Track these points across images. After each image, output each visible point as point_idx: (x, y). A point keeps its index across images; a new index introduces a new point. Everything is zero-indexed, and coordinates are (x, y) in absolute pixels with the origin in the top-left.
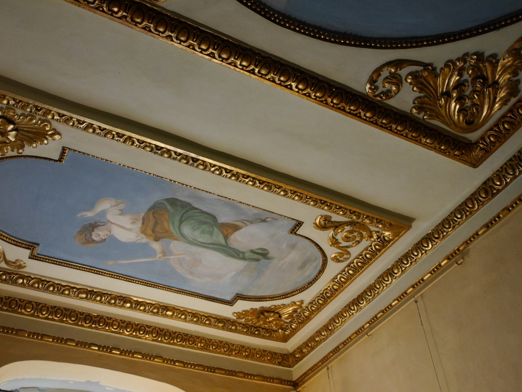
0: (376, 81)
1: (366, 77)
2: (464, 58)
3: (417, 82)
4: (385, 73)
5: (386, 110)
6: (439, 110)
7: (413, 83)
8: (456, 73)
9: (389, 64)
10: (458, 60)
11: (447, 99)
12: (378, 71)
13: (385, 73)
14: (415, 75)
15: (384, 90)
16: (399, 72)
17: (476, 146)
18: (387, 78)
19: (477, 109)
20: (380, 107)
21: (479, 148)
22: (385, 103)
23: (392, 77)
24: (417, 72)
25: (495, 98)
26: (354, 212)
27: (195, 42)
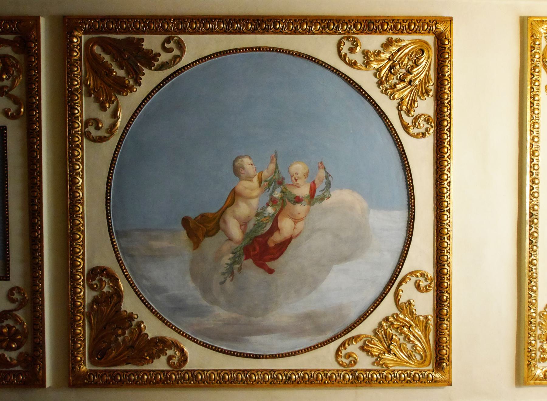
0: (423, 134)
1: (423, 140)
2: (385, 92)
3: (412, 108)
4: (415, 131)
5: (438, 114)
6: (423, 79)
7: (413, 110)
8: (395, 89)
9: (408, 133)
10: (387, 95)
11: (413, 81)
12: (416, 136)
13: (415, 131)
14: (408, 112)
15: (425, 123)
16: (411, 124)
17: (436, 33)
18: (417, 128)
19: (411, 56)
20: (438, 118)
21: (436, 30)
22: (434, 117)
23: (415, 125)
24: (405, 112)
25: (398, 51)
26: (531, 74)
27: (445, 251)
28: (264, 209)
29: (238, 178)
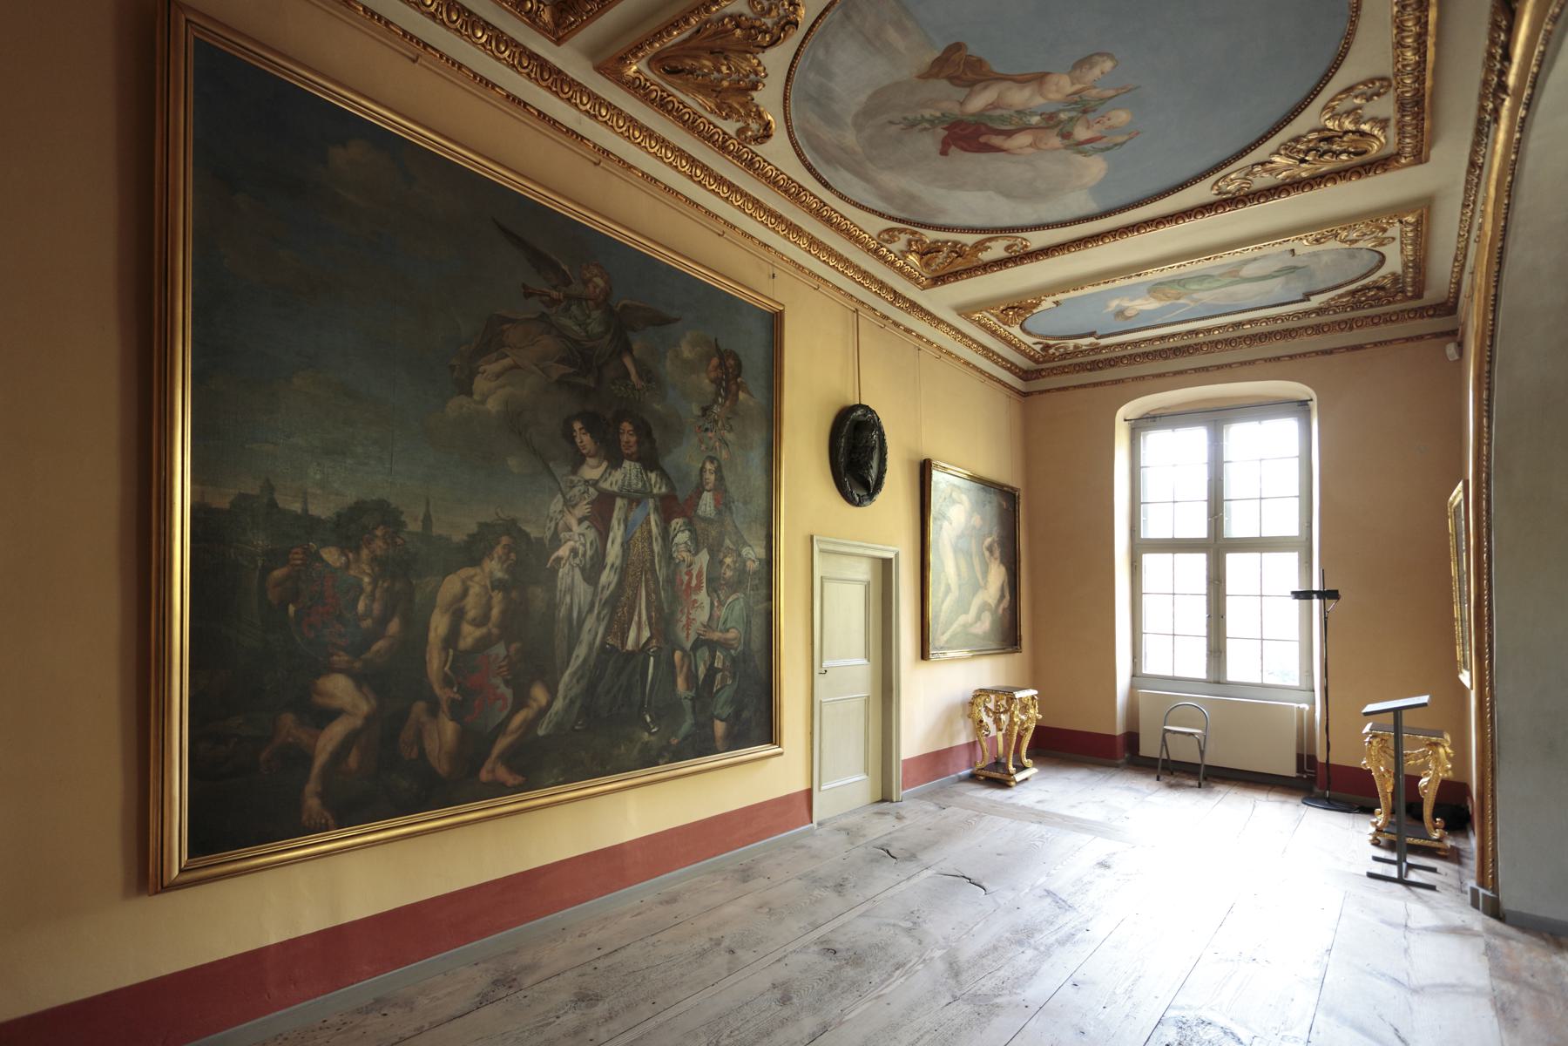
28: (1033, 113)
29: (1070, 69)
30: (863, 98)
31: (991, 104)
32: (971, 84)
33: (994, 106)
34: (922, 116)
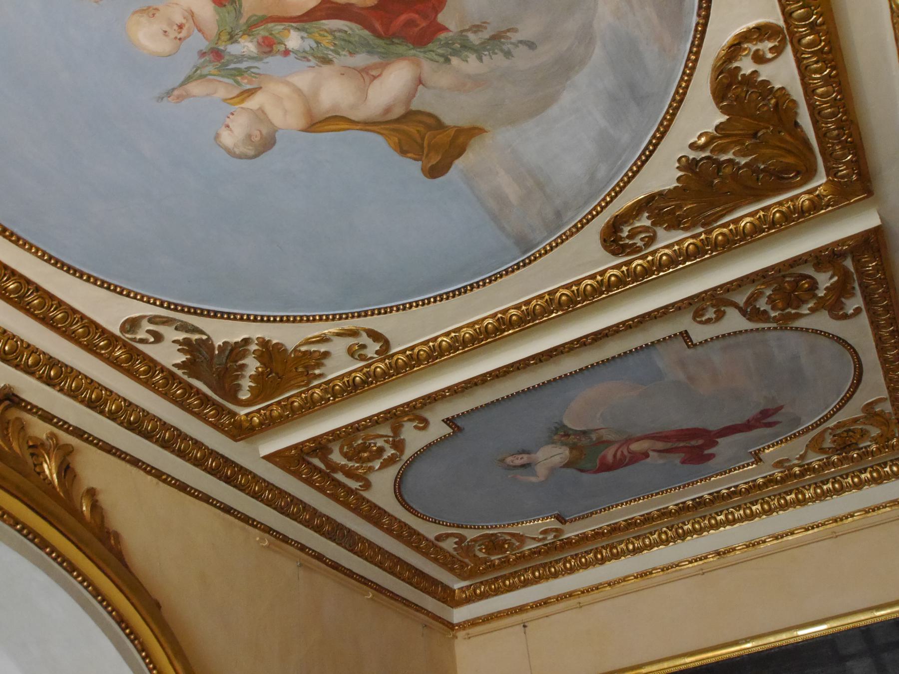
30: (567, 98)
31: (375, 78)
32: (409, 116)
33: (368, 75)
34: (480, 59)
